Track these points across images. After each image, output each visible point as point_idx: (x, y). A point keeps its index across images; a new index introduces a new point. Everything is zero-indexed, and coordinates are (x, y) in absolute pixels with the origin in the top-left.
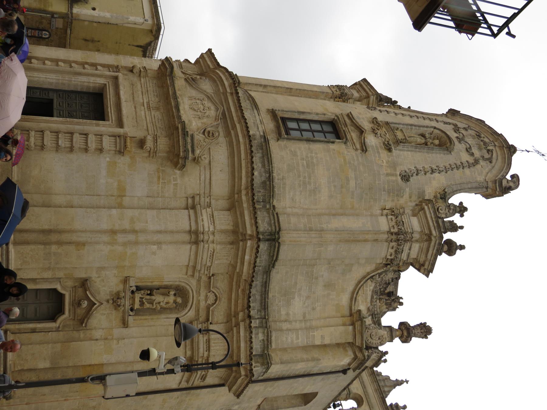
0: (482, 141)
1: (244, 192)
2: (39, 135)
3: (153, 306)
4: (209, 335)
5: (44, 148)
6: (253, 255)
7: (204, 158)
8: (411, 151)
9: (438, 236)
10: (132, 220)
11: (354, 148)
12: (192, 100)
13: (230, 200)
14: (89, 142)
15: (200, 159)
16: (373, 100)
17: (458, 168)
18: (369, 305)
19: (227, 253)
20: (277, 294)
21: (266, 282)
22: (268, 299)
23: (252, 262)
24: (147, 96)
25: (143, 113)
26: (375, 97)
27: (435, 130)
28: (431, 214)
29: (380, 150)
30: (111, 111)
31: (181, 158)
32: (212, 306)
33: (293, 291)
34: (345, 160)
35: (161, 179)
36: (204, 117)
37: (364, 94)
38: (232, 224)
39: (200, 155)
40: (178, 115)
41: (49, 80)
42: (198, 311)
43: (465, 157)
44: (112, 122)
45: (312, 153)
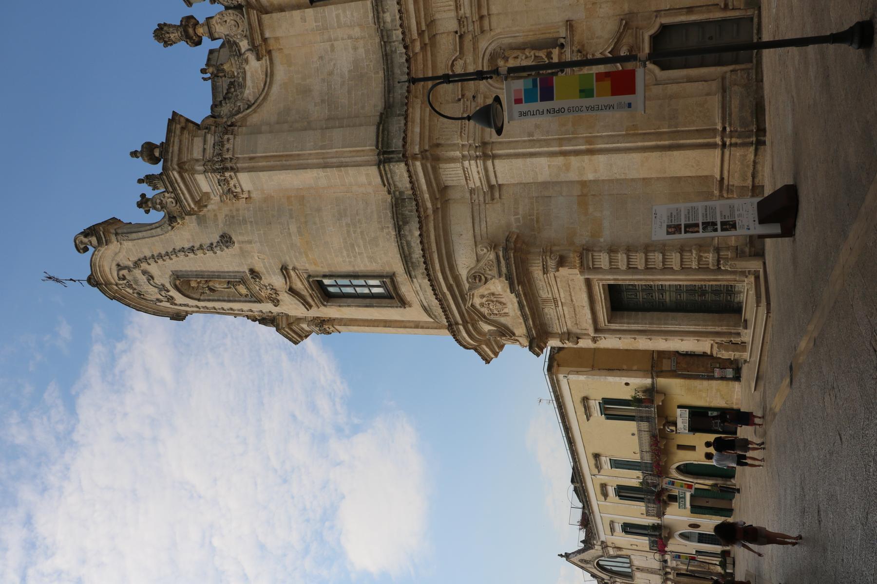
0: (135, 289)
1: (430, 211)
2: (687, 264)
3: (534, 54)
4: (457, 16)
5: (680, 249)
6: (409, 134)
8: (222, 272)
9: (170, 172)
10: (567, 167)
11: (298, 270)
12: (504, 313)
13: (447, 199)
14: (625, 260)
15: (489, 249)
16: (282, 322)
17: (160, 256)
18: (247, 68)
19: (444, 132)
20: (373, 76)
21: (389, 92)
22: (384, 68)
23: (410, 124)
25: (562, 295)
26: (281, 326)
27: (199, 298)
29: (265, 270)
31: (512, 249)
32: (456, 57)
33: (352, 81)
34: (307, 256)
35: (535, 219)
36: (488, 296)
37: (294, 327)
39: (489, 253)
41: (677, 323)
42: (475, 48)
43: (153, 268)
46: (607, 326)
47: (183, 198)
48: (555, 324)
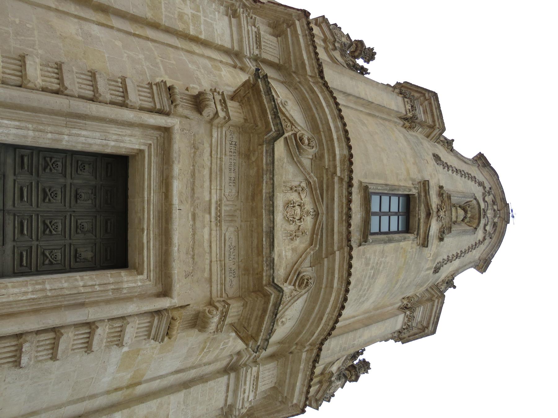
7: (282, 322)
14: (95, 342)
16: (436, 134)
24: (218, 183)
25: (206, 231)
27: (474, 200)
28: (437, 309)
30: (148, 242)
37: (430, 121)
38: (275, 380)
40: (270, 257)
44: (148, 277)
45: (383, 257)
46: (145, 144)
47: (438, 309)
48: (228, 153)
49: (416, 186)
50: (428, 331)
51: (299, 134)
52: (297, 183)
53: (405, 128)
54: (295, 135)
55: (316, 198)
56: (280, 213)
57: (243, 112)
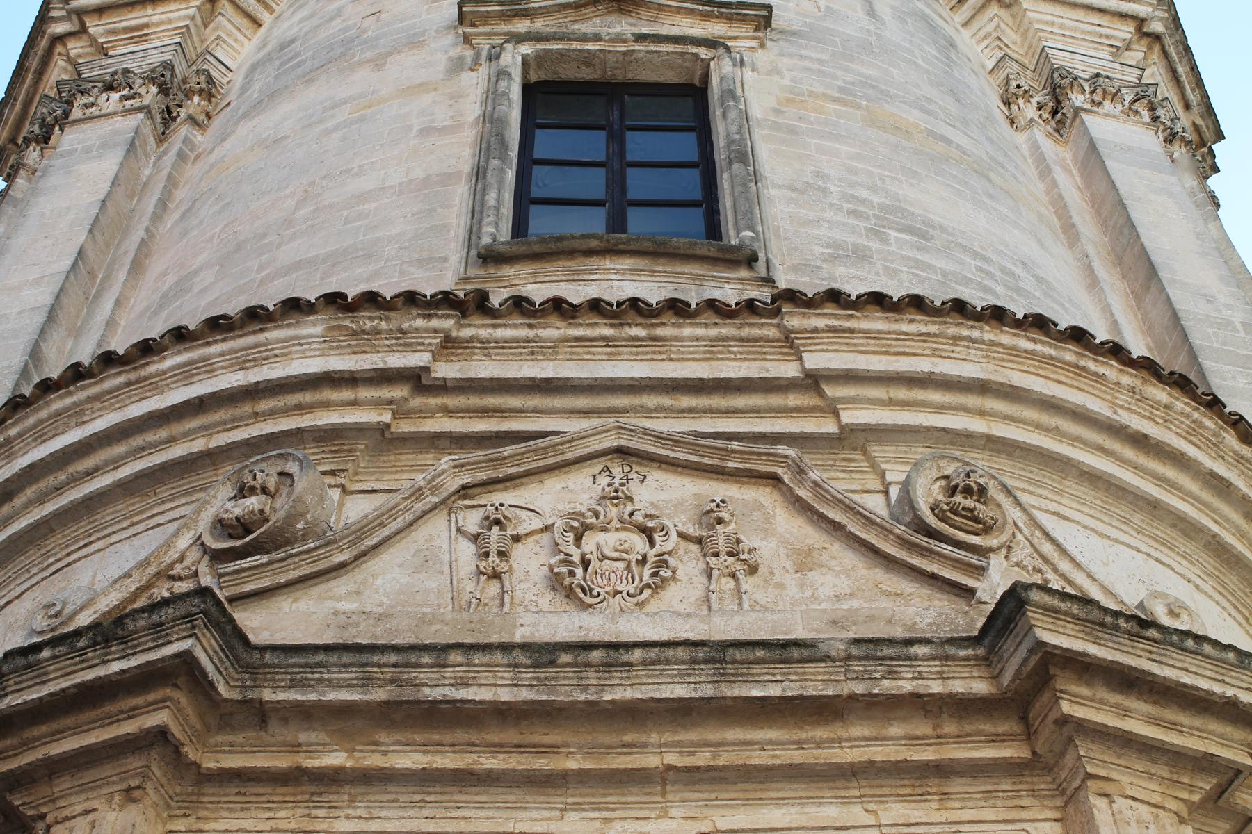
45: (824, 191)
49: (484, 54)
50: (1161, 19)
51: (216, 539)
52: (466, 550)
53: (209, 116)
54: (218, 557)
55: (541, 463)
56: (621, 628)
57: (87, 812)
